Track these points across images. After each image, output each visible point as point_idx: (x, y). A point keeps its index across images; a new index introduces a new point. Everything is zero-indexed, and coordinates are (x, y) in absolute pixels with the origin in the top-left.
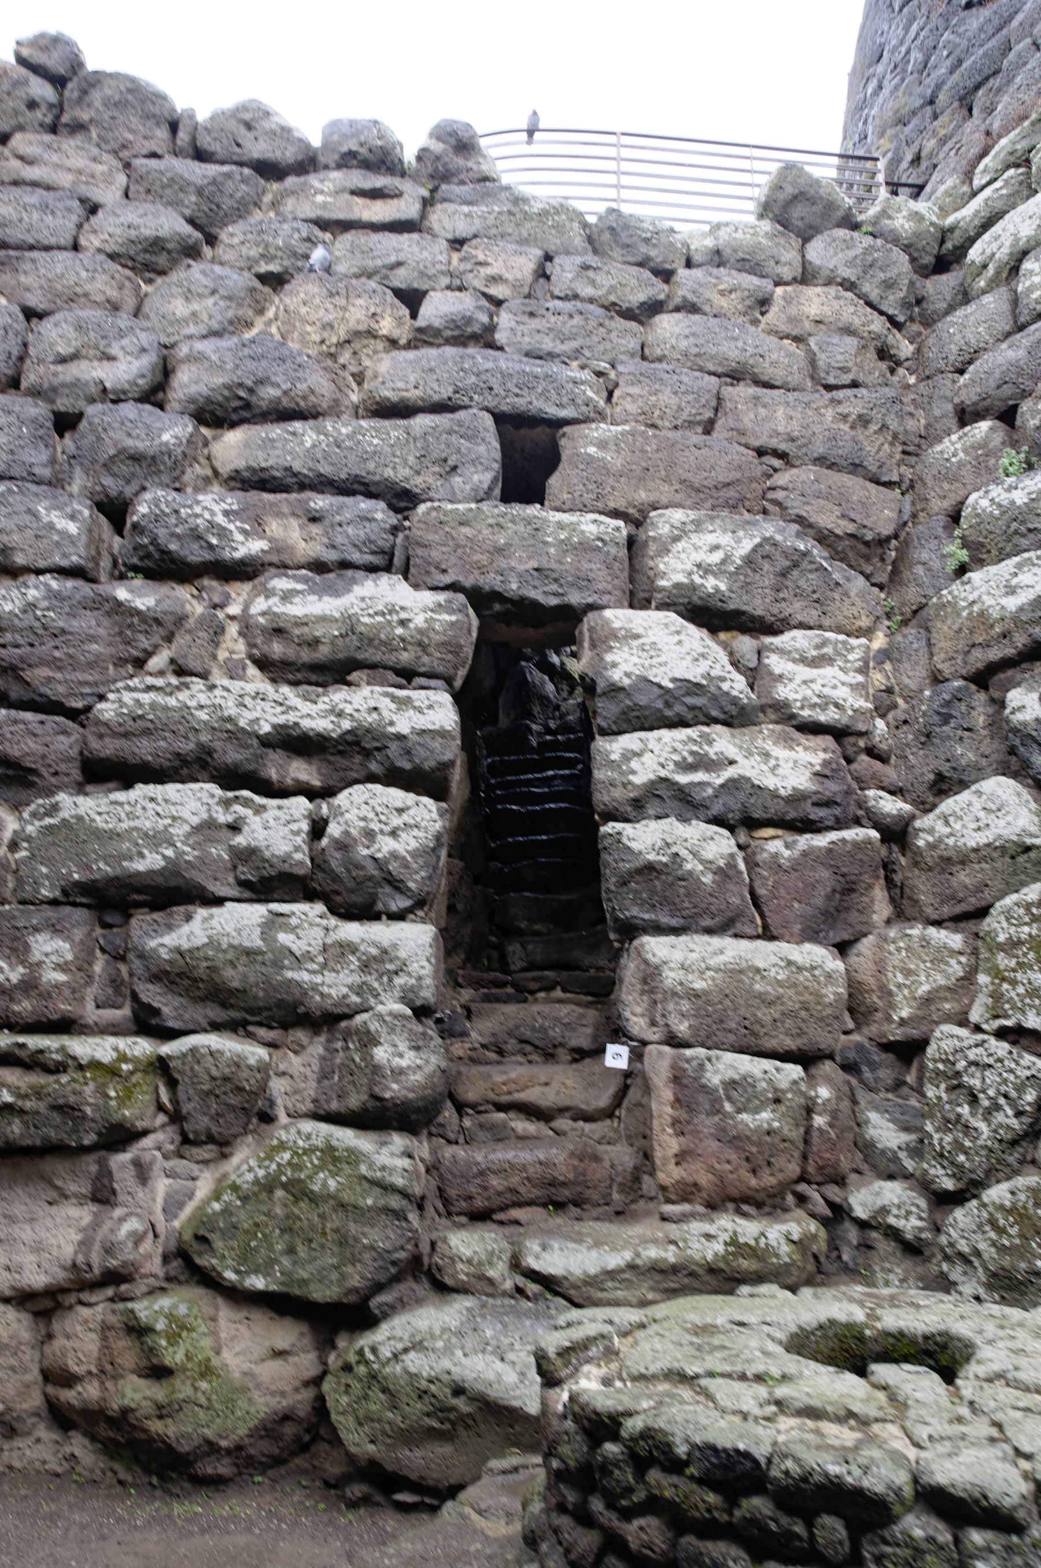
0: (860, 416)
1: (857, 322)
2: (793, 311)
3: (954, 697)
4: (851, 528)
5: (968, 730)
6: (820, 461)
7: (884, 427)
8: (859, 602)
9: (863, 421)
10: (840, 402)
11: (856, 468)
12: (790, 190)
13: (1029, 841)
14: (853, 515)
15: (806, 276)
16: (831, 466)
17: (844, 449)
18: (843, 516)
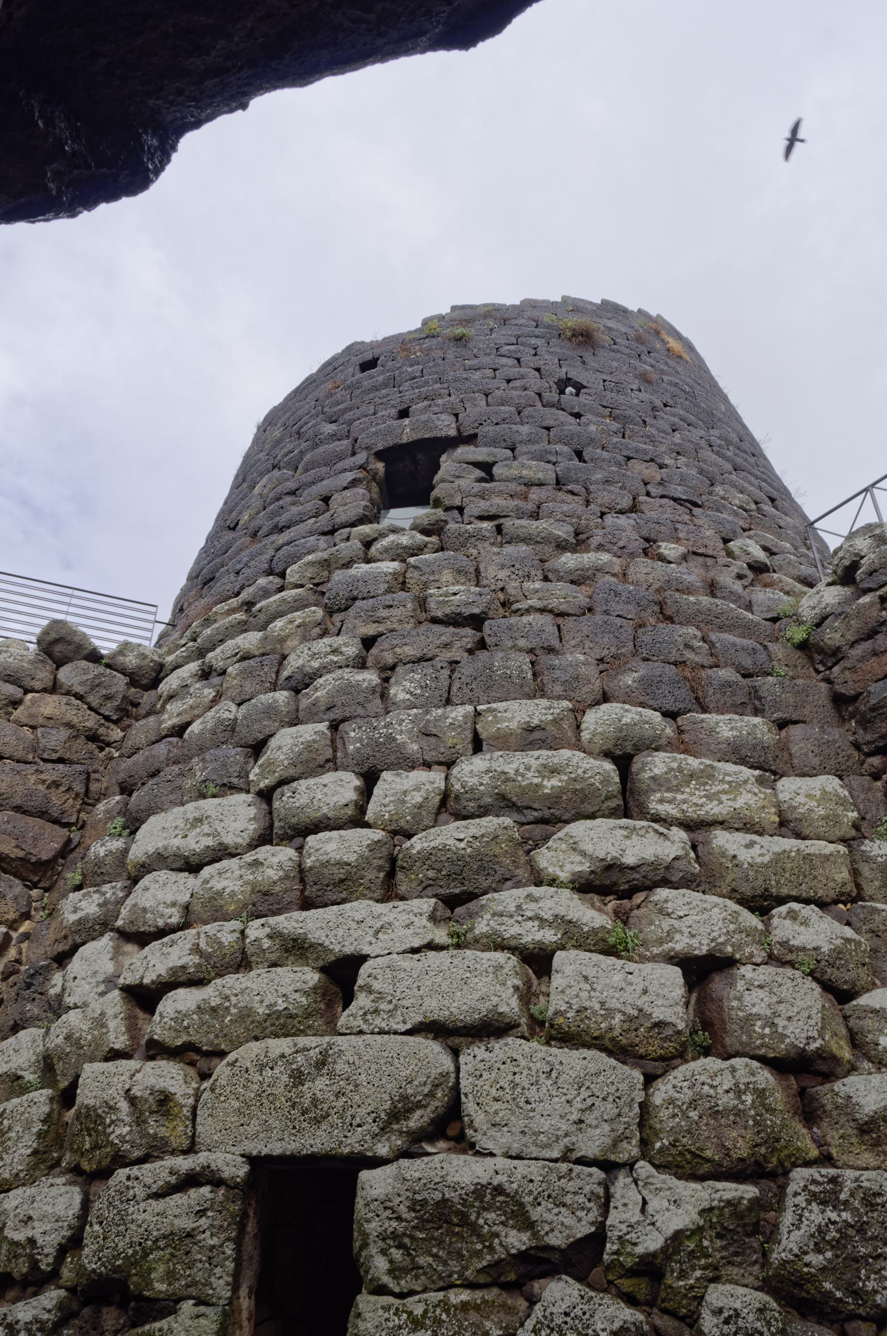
0: (54, 782)
1: (75, 720)
2: (33, 710)
3: (37, 972)
4: (21, 854)
5: (41, 994)
6: (18, 809)
7: (69, 789)
8: (10, 903)
9: (56, 784)
10: (42, 772)
11: (42, 814)
12: (54, 636)
13: (20, 1073)
14: (23, 847)
15: (54, 688)
16: (24, 812)
17: (36, 802)
18: (17, 847)
